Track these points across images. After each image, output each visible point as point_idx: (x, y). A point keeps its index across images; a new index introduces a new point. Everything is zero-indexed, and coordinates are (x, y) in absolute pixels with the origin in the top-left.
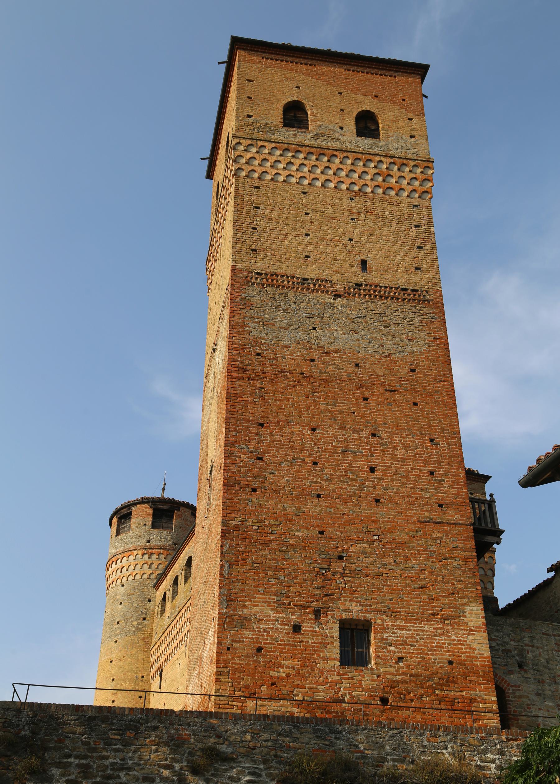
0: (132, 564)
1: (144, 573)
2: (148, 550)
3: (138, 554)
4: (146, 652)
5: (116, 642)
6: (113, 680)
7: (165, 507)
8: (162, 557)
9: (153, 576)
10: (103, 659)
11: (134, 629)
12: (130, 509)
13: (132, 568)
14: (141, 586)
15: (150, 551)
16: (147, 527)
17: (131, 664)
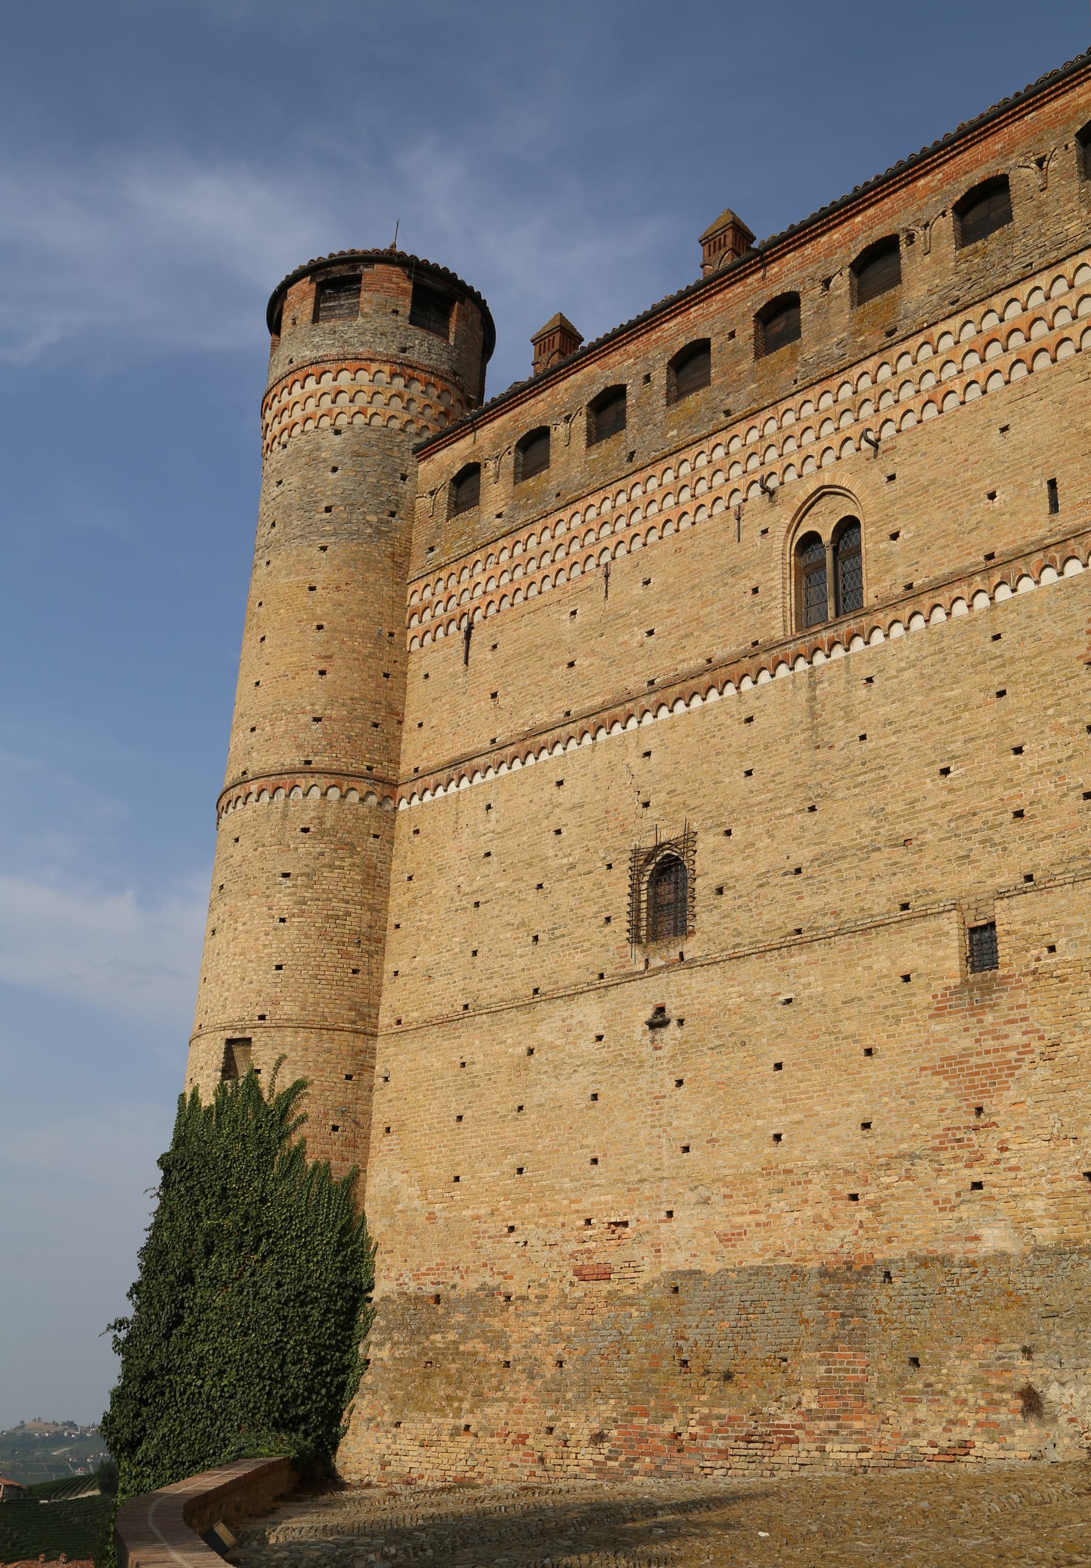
0: (363, 388)
1: (393, 417)
2: (405, 369)
3: (379, 371)
4: (397, 584)
5: (324, 549)
6: (320, 627)
7: (439, 287)
8: (434, 392)
9: (412, 428)
10: (283, 581)
11: (369, 531)
12: (355, 268)
13: (362, 399)
14: (384, 442)
15: (409, 371)
16: (399, 318)
17: (363, 601)
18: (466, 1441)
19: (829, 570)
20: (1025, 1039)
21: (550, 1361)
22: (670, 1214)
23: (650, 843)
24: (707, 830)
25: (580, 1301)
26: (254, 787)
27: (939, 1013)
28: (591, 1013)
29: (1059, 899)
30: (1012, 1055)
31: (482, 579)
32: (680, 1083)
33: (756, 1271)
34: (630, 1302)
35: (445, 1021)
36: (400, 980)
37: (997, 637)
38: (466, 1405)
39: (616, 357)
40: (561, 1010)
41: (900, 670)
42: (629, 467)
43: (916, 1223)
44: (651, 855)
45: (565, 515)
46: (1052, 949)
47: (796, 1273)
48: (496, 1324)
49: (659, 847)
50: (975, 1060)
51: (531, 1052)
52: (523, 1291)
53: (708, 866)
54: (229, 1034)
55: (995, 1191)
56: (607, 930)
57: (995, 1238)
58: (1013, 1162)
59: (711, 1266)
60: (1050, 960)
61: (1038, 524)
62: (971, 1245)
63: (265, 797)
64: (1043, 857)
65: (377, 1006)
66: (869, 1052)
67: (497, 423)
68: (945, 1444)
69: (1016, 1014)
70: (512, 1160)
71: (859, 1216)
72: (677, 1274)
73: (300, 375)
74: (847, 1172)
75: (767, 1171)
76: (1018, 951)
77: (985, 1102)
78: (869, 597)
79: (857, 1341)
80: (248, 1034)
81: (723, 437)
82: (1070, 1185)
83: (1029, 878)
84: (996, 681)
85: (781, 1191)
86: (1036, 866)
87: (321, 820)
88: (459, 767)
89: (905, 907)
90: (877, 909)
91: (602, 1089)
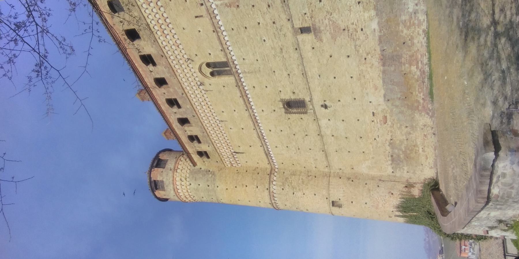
2: (175, 170)
8: (180, 163)
18: (426, 149)
19: (218, 69)
20: (327, 20)
21: (406, 129)
22: (370, 102)
23: (283, 110)
24: (280, 96)
25: (392, 123)
26: (273, 201)
27: (321, 40)
28: (323, 122)
29: (293, 12)
30: (331, 22)
31: (223, 150)
32: (339, 101)
33: (384, 82)
34: (392, 111)
35: (326, 156)
36: (317, 166)
37: (233, 29)
38: (417, 149)
39: (171, 121)
40: (323, 129)
41: (241, 52)
42: (196, 117)
43: (371, 43)
44: (286, 109)
45: (208, 131)
46: (305, 14)
47: (384, 72)
48: (398, 142)
49: (284, 107)
50: (332, 32)
51: (333, 136)
52: (390, 136)
53: (288, 96)
54: (331, 206)
55: (363, 25)
56: (304, 119)
57: (374, 25)
58: (356, 21)
59: (383, 92)
60: (308, 14)
61: (206, 20)
62: (376, 31)
63: (275, 199)
64: (284, 17)
65: (323, 172)
66: (331, 56)
67: (187, 148)
68: (423, 36)
69: (321, 22)
70: (359, 139)
71: (370, 58)
72: (384, 100)
73: (177, 194)
74: (360, 61)
75: (359, 79)
76: (306, 22)
77: (342, 29)
78: (224, 60)
79: (400, 57)
80: (331, 202)
81: (188, 95)
82: (361, 7)
83: (289, 20)
84: (243, 29)
85: (364, 76)
86: (286, 18)
87: (280, 186)
88: (267, 154)
89: (296, 49)
90: (297, 56)
91: (341, 119)
